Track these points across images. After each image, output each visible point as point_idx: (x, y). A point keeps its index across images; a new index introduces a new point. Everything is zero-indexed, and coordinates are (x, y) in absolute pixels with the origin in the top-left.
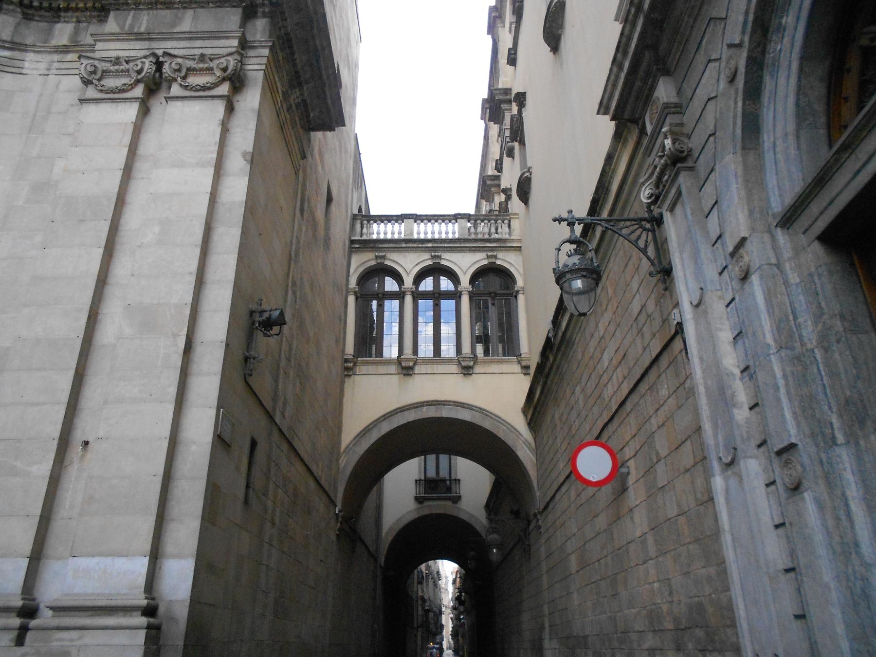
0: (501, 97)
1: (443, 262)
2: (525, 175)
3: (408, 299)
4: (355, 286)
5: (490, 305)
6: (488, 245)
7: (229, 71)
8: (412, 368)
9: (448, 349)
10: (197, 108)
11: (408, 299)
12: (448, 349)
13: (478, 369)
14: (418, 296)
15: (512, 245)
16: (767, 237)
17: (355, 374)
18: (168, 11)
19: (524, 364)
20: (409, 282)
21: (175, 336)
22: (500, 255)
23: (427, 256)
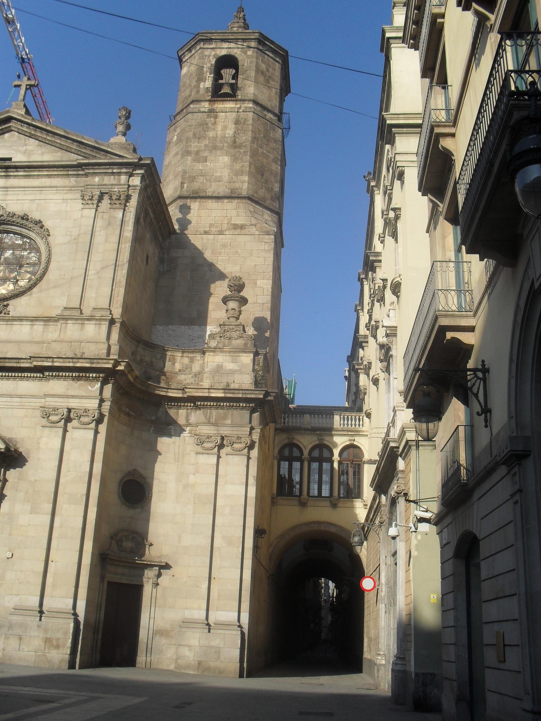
0: (362, 340)
1: (325, 442)
2: (368, 411)
3: (306, 464)
4: (277, 455)
5: (349, 467)
6: (350, 433)
7: (248, 445)
8: (306, 503)
9: (325, 492)
10: (237, 459)
11: (306, 464)
12: (325, 492)
13: (340, 505)
14: (312, 460)
15: (363, 434)
16: (389, 558)
17: (277, 504)
18: (222, 410)
19: (365, 503)
20: (306, 453)
21: (238, 547)
22: (357, 438)
23: (315, 438)
